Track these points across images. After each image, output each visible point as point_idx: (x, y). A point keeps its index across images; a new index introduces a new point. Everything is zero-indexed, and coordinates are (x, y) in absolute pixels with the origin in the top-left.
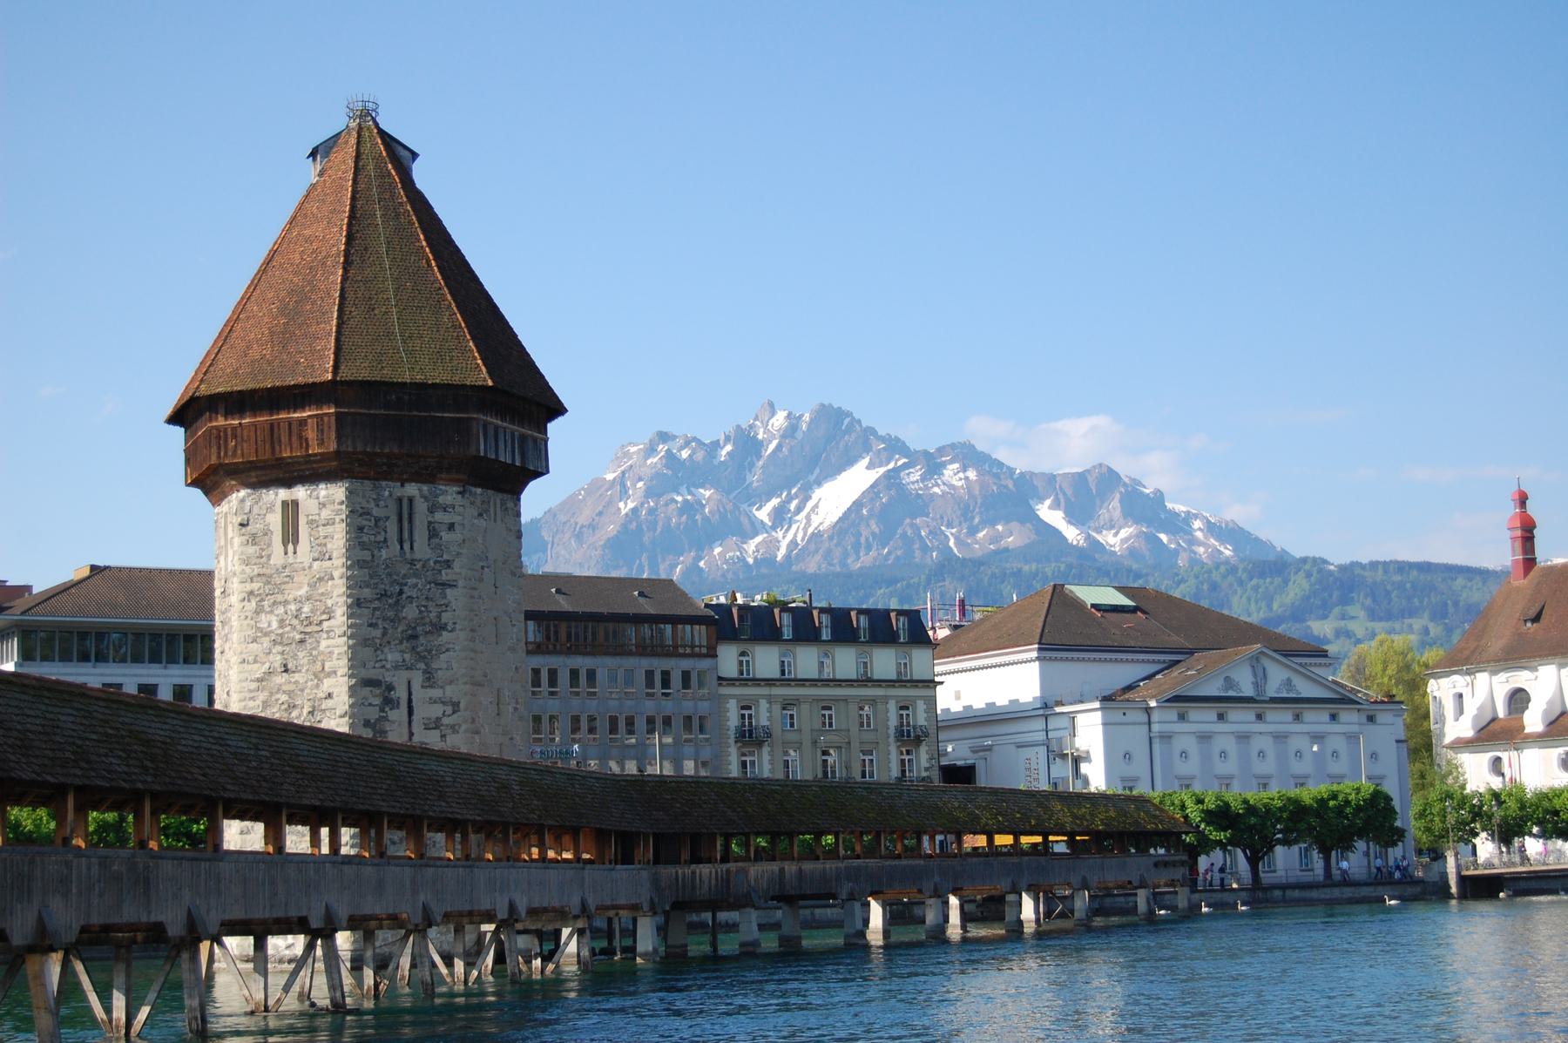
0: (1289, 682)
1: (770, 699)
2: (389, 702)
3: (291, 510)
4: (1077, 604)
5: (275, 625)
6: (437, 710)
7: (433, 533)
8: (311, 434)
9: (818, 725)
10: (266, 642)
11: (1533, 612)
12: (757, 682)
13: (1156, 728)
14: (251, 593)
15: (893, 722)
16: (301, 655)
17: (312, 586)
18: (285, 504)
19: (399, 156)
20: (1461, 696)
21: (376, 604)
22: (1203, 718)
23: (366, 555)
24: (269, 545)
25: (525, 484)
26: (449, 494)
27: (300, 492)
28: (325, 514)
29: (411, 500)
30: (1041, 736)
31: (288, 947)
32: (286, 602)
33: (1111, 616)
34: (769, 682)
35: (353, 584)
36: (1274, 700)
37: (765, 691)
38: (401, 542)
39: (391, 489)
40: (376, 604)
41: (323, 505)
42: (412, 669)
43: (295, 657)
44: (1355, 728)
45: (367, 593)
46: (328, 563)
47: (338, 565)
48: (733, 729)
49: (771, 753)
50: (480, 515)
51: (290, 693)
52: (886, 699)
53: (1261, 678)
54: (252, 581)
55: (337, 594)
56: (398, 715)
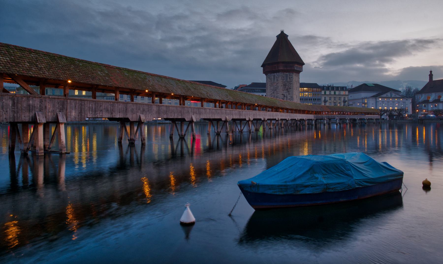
0: (395, 95)
1: (328, 97)
2: (285, 97)
3: (274, 76)
5: (272, 88)
6: (289, 98)
7: (290, 78)
9: (333, 100)
12: (326, 95)
14: (270, 85)
15: (343, 99)
17: (276, 84)
18: (274, 75)
19: (286, 36)
20: (420, 97)
23: (282, 81)
25: (300, 72)
26: (291, 74)
27: (275, 74)
28: (278, 76)
30: (362, 101)
32: (274, 86)
34: (328, 95)
36: (393, 97)
37: (327, 96)
38: (286, 79)
39: (285, 73)
41: (278, 75)
42: (287, 93)
43: (274, 92)
44: (404, 101)
45: (282, 85)
46: (278, 82)
48: (323, 100)
49: (328, 103)
50: (295, 76)
51: (274, 96)
52: (342, 97)
54: (270, 83)
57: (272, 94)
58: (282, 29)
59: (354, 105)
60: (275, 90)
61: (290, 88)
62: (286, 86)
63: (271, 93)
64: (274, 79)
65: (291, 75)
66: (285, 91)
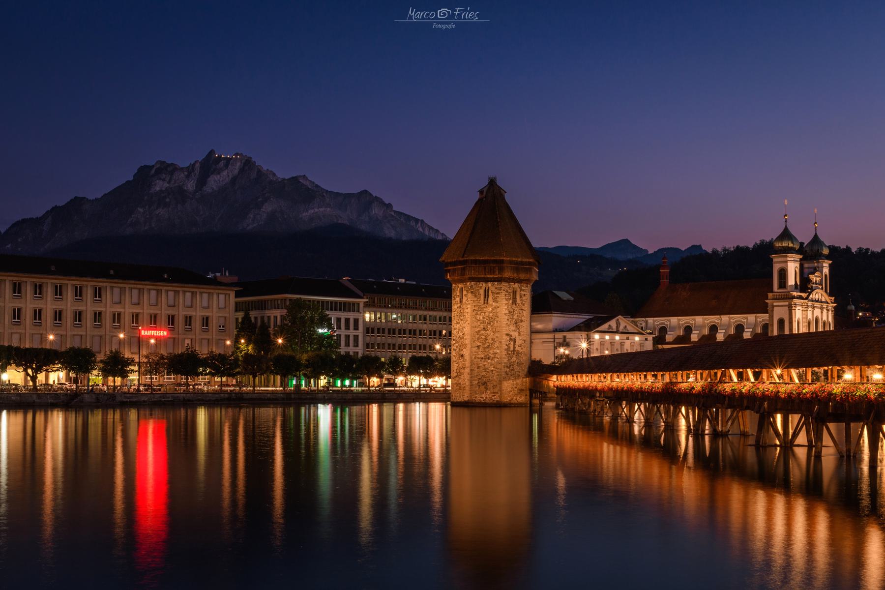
0: (626, 327)
5: (481, 318)
6: (520, 342)
7: (521, 297)
10: (479, 323)
16: (489, 326)
17: (492, 309)
21: (509, 314)
24: (480, 297)
27: (490, 284)
29: (516, 288)
31: (484, 400)
40: (509, 314)
41: (496, 288)
45: (507, 312)
53: (618, 324)
57: (479, 331)
60: (490, 323)
61: (522, 321)
62: (513, 315)
63: (479, 329)
64: (485, 295)
65: (523, 290)
66: (512, 328)
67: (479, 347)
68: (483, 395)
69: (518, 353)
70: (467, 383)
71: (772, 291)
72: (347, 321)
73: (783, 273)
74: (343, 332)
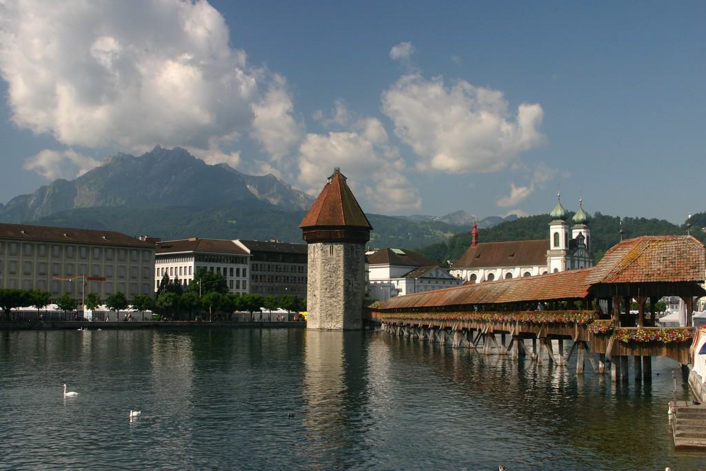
2: (350, 284)
4: (393, 253)
8: (339, 234)
11: (478, 255)
13: (416, 284)
14: (323, 262)
20: (459, 275)
22: (425, 282)
26: (359, 246)
33: (401, 257)
35: (344, 262)
36: (440, 279)
39: (350, 245)
47: (342, 258)
53: (437, 273)
55: (341, 263)
56: (351, 286)
57: (327, 277)
58: (337, 166)
59: (372, 291)
61: (357, 270)
66: (350, 275)
67: (326, 289)
68: (330, 324)
69: (355, 294)
70: (318, 314)
71: (549, 249)
72: (238, 270)
73: (556, 235)
74: (235, 278)
